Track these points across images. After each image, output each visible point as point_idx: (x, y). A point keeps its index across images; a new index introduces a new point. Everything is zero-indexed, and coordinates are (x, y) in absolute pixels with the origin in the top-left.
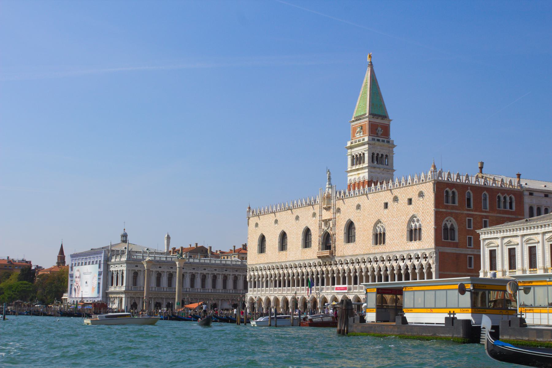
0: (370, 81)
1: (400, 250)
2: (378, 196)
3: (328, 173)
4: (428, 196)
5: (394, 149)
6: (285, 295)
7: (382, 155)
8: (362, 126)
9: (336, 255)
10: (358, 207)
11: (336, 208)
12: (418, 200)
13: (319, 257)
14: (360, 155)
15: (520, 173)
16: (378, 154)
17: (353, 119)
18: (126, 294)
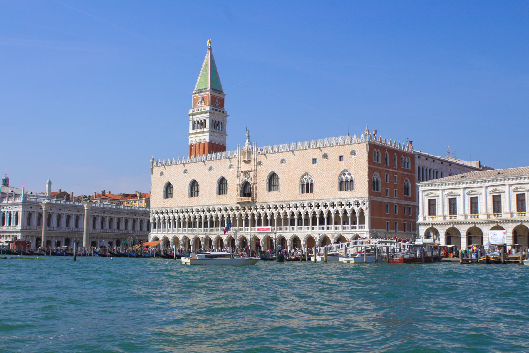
0: (210, 62)
1: (330, 198)
2: (306, 153)
3: (248, 132)
4: (361, 155)
5: (227, 118)
6: (197, 234)
7: (219, 122)
8: (203, 98)
10: (283, 161)
11: (257, 162)
12: (350, 157)
13: (238, 203)
14: (201, 121)
15: (411, 141)
16: (216, 121)
17: (195, 92)
18: (22, 233)
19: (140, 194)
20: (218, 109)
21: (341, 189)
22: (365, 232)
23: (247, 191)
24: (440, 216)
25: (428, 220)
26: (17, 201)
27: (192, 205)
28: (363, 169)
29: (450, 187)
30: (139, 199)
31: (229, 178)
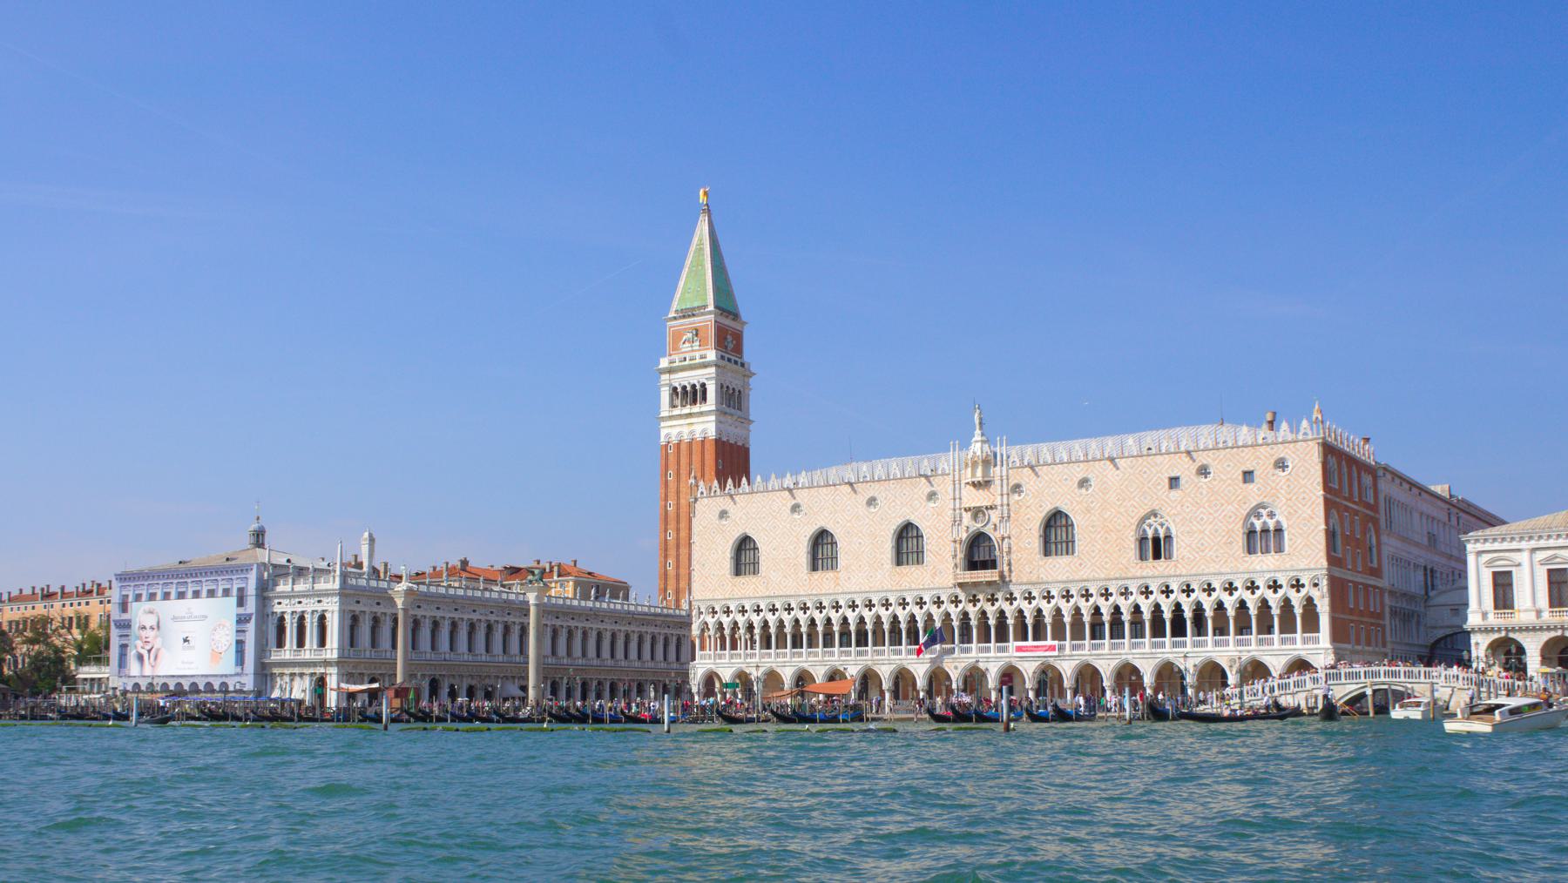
1: (1223, 570)
3: (978, 411)
4: (1303, 468)
8: (697, 330)
9: (1014, 580)
10: (1083, 483)
11: (1011, 485)
13: (961, 585)
14: (694, 386)
17: (672, 315)
19: (559, 565)
20: (733, 358)
21: (1251, 550)
22: (1322, 651)
23: (981, 556)
24: (1526, 611)
25: (1493, 620)
26: (321, 586)
27: (819, 592)
28: (1310, 503)
29: (1552, 542)
30: (555, 578)
31: (928, 524)
